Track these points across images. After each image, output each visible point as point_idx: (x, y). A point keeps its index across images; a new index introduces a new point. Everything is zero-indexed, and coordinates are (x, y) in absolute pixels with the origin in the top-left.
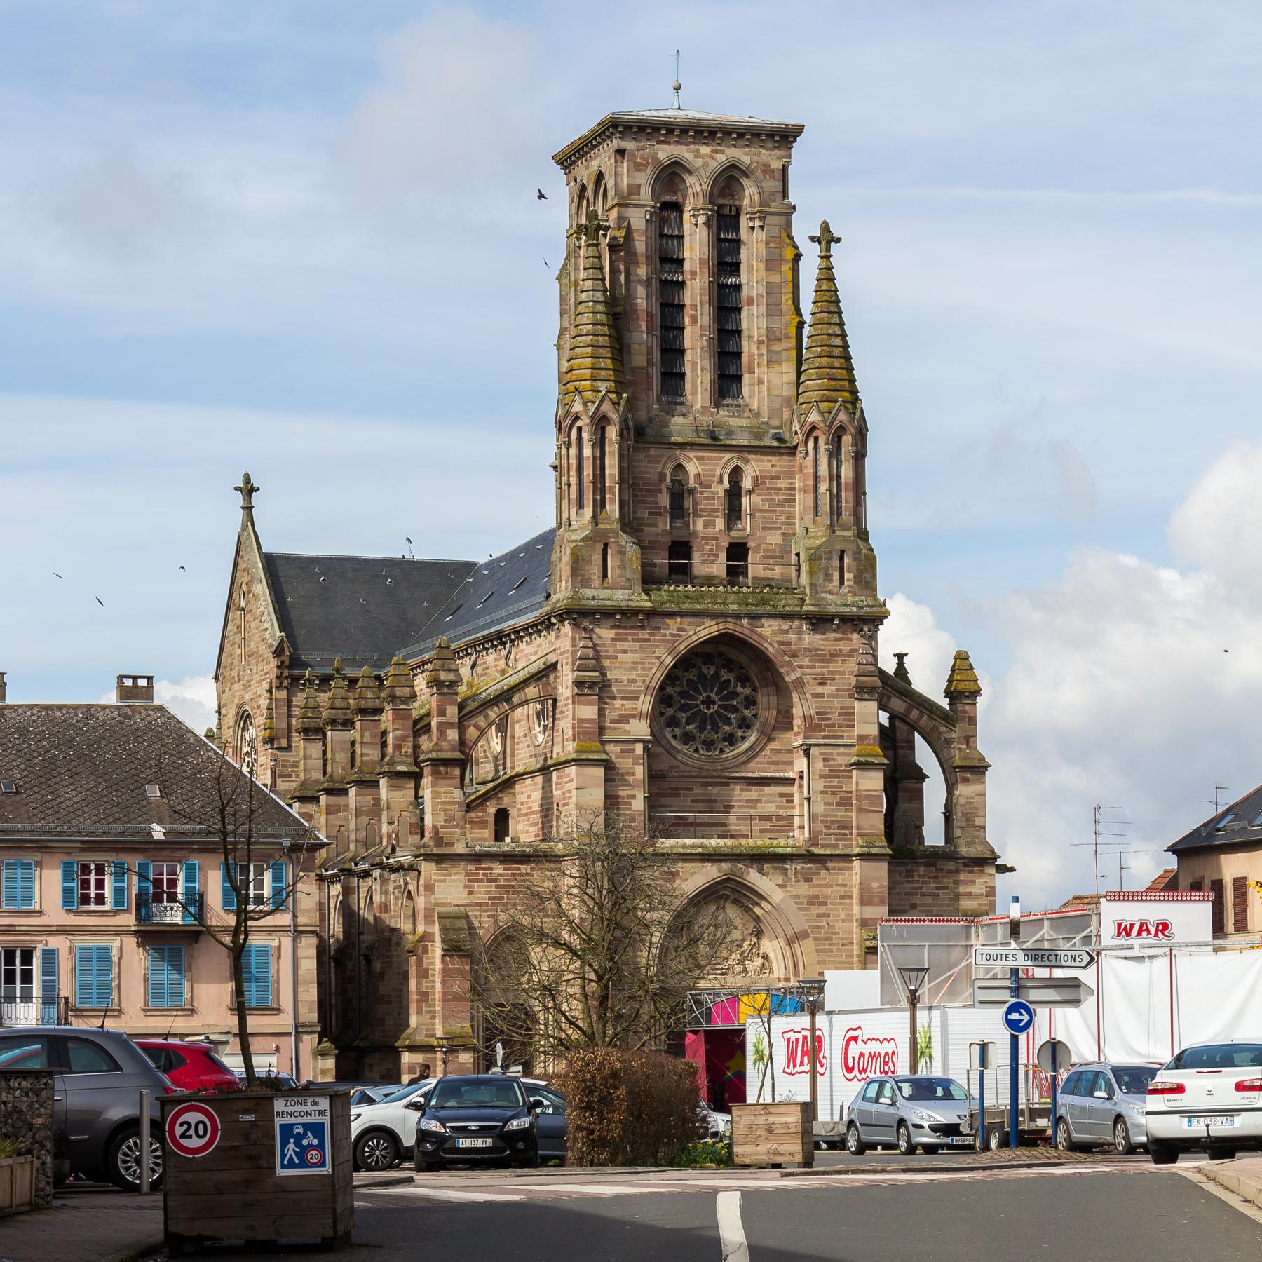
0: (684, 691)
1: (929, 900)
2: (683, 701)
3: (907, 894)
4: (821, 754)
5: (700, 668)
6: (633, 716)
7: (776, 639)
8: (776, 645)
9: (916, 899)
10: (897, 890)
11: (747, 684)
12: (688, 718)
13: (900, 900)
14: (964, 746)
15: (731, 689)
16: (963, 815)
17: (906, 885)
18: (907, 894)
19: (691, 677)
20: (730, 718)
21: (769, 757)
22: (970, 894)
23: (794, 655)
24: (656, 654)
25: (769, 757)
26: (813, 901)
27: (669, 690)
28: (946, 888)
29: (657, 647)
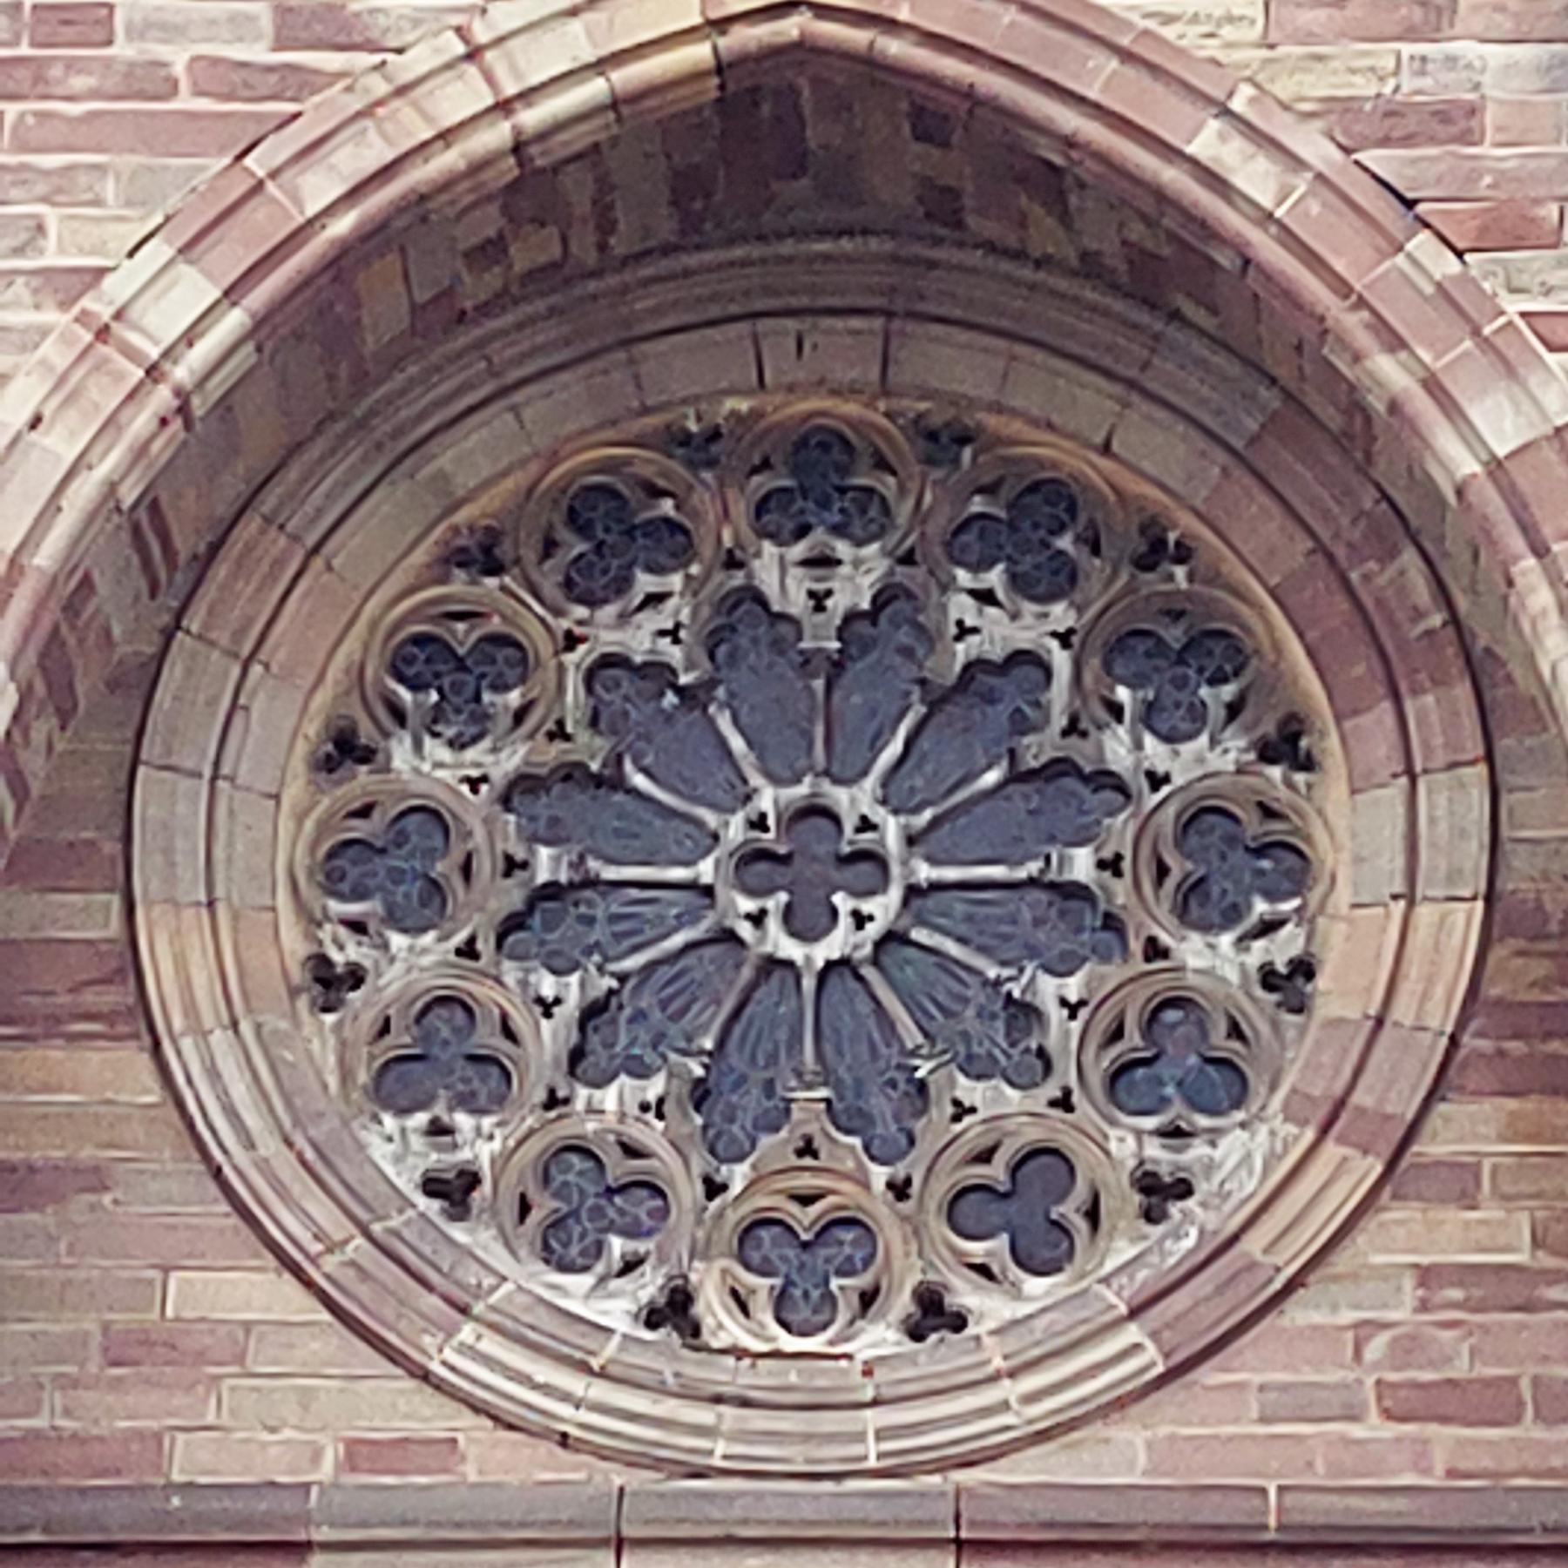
0: (571, 773)
2: (546, 865)
5: (733, 562)
7: (1317, 86)
8: (1315, 147)
11: (1217, 697)
12: (592, 1012)
15: (1038, 749)
19: (639, 641)
20: (1024, 1013)
21: (1408, 1348)
24: (51, 258)
25: (1408, 1348)
29: (59, 188)
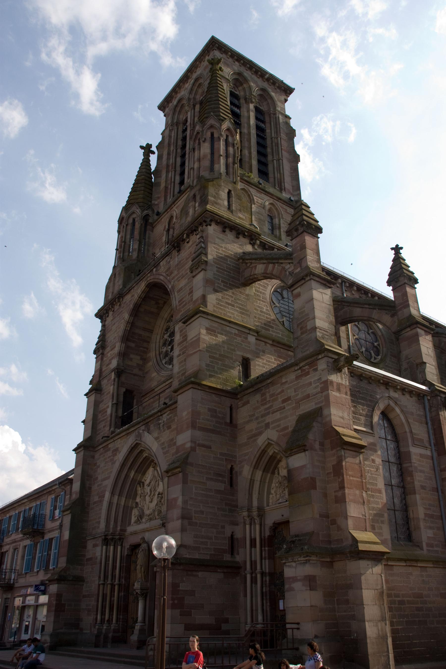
1: (278, 415)
3: (262, 416)
4: (179, 328)
6: (112, 358)
9: (269, 419)
10: (257, 415)
13: (258, 423)
14: (299, 269)
16: (298, 326)
17: (262, 408)
18: (262, 416)
22: (308, 396)
23: (172, 273)
26: (172, 442)
27: (166, 336)
28: (289, 399)
